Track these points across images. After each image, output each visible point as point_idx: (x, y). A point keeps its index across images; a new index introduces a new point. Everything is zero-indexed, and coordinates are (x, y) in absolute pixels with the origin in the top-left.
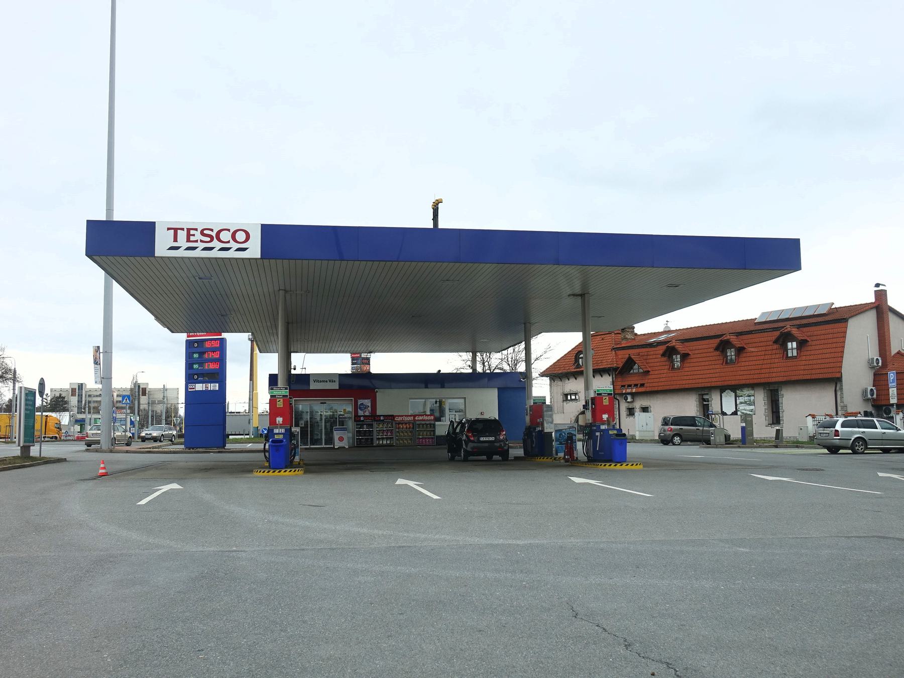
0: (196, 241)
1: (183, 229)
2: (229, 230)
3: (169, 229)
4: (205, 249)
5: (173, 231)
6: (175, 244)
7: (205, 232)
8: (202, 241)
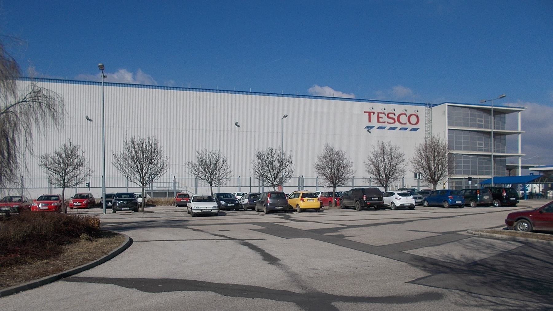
0: (384, 122)
3: (365, 112)
4: (391, 128)
5: (368, 114)
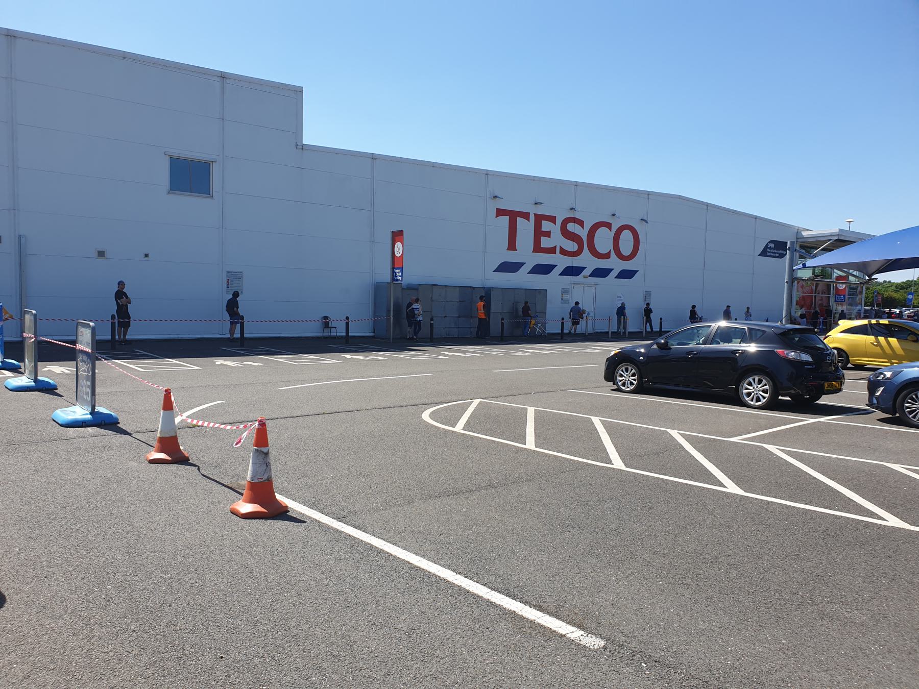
0: (552, 250)
1: (526, 216)
2: (608, 225)
3: (500, 212)
6: (512, 257)
7: (571, 227)
8: (564, 252)
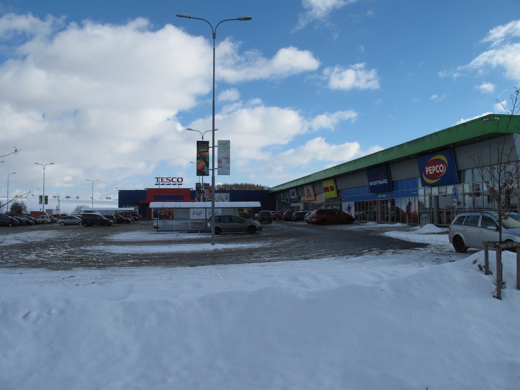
0: (165, 182)
2: (176, 178)
3: (155, 178)
5: (156, 179)
6: (158, 183)
7: (168, 179)
8: (167, 182)
